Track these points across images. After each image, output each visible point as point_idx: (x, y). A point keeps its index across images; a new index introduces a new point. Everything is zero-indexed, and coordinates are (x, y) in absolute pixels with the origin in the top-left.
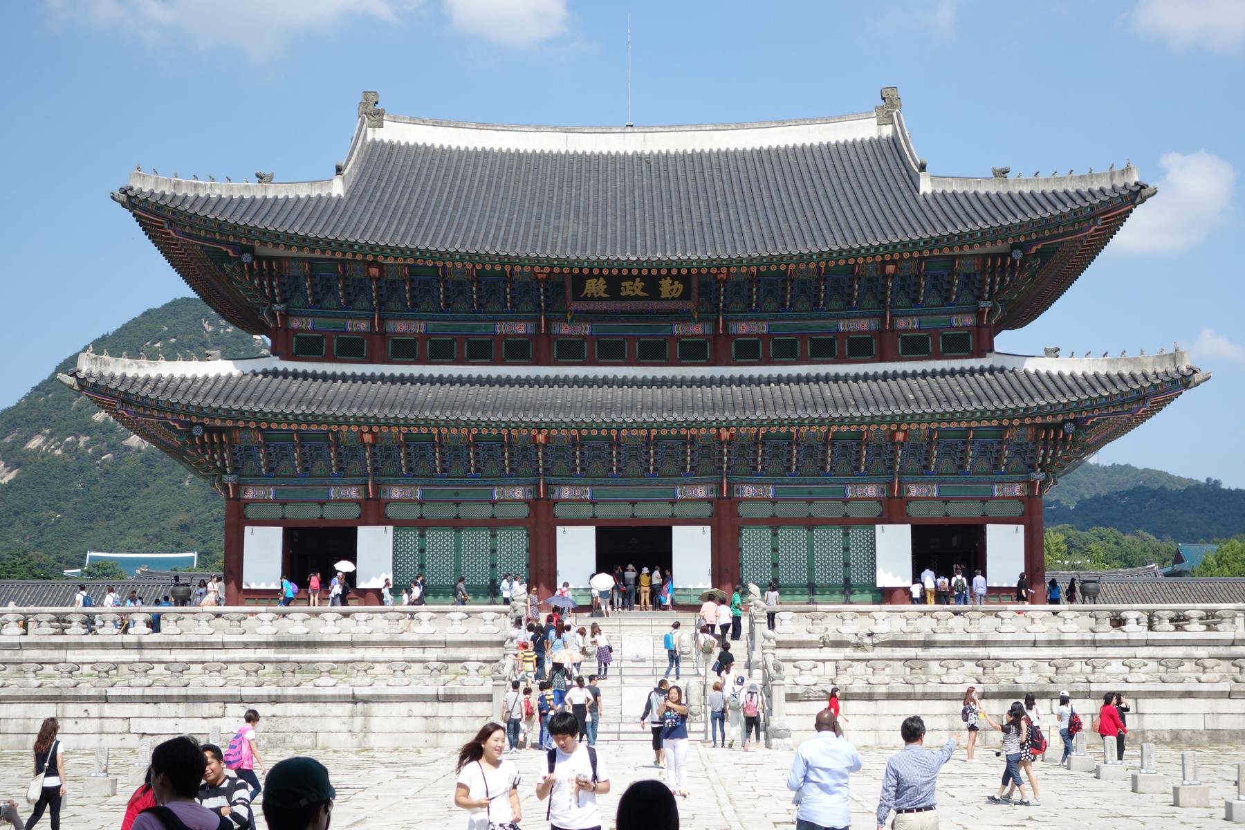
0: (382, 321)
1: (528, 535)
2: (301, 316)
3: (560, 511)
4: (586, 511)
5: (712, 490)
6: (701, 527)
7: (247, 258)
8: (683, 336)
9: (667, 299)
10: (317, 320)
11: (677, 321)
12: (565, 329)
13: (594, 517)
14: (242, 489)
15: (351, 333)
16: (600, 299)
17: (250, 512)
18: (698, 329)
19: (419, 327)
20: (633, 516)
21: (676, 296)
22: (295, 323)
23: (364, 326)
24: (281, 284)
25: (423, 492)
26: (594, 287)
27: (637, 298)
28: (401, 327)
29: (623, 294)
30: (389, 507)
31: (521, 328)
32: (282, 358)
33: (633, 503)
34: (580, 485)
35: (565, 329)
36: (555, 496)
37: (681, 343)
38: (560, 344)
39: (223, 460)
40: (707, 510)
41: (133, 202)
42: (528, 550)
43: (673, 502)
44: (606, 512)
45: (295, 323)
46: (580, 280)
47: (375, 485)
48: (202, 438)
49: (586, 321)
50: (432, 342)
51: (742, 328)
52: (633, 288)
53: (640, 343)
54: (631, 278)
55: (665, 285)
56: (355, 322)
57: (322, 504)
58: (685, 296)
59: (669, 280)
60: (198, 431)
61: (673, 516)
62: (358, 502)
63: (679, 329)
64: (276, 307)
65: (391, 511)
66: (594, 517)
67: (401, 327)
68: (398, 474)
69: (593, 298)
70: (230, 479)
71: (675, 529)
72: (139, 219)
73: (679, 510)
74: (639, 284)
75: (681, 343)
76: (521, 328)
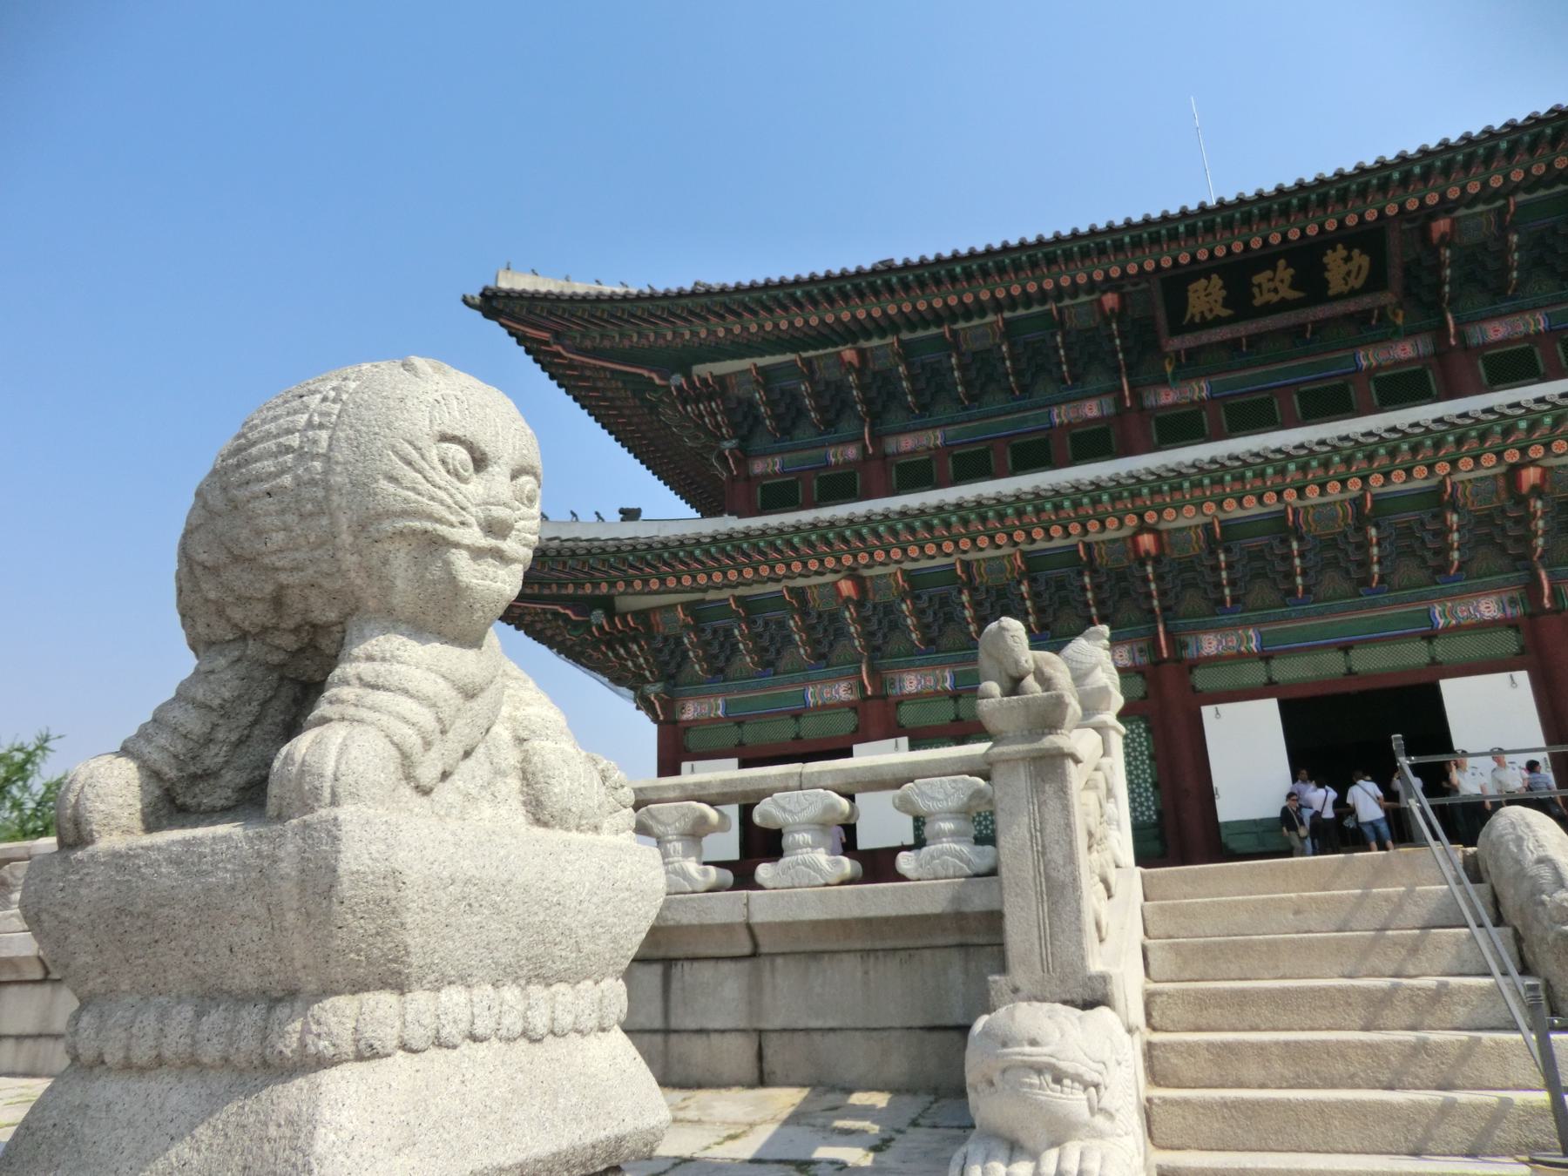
0: (877, 438)
1: (1148, 730)
2: (764, 454)
3: (1203, 679)
4: (1255, 674)
5: (1513, 602)
6: (1504, 676)
7: (677, 379)
8: (1379, 367)
9: (1340, 297)
10: (787, 456)
11: (1364, 344)
12: (1166, 397)
13: (1271, 682)
14: (678, 709)
15: (837, 464)
16: (1219, 322)
17: (692, 740)
18: (1404, 350)
19: (935, 438)
20: (1350, 672)
21: (1357, 283)
22: (758, 467)
23: (852, 452)
24: (728, 412)
25: (955, 676)
26: (1205, 297)
27: (1284, 306)
28: (907, 443)
29: (1257, 302)
30: (903, 708)
31: (1091, 409)
32: (740, 517)
33: (1346, 648)
34: (1234, 626)
35: (1166, 397)
36: (1190, 653)
37: (1378, 381)
38: (1159, 421)
39: (633, 656)
40: (1508, 643)
41: (494, 304)
42: (1152, 757)
43: (1429, 637)
44: (1291, 670)
45: (758, 467)
46: (1176, 283)
47: (873, 672)
48: (600, 628)
49: (1197, 376)
50: (955, 458)
51: (1496, 331)
52: (1274, 284)
53: (1302, 396)
54: (1267, 259)
55: (1334, 259)
56: (841, 449)
57: (797, 716)
58: (1375, 281)
59: (1341, 251)
60: (598, 617)
61: (1433, 662)
62: (852, 706)
63: (1367, 358)
64: (727, 445)
65: (907, 715)
66: (1271, 682)
67: (907, 443)
68: (912, 651)
69: (1206, 324)
70: (653, 690)
71: (1448, 687)
72: (535, 350)
73: (1442, 650)
74: (1285, 272)
75: (1378, 381)
76: (1091, 409)
